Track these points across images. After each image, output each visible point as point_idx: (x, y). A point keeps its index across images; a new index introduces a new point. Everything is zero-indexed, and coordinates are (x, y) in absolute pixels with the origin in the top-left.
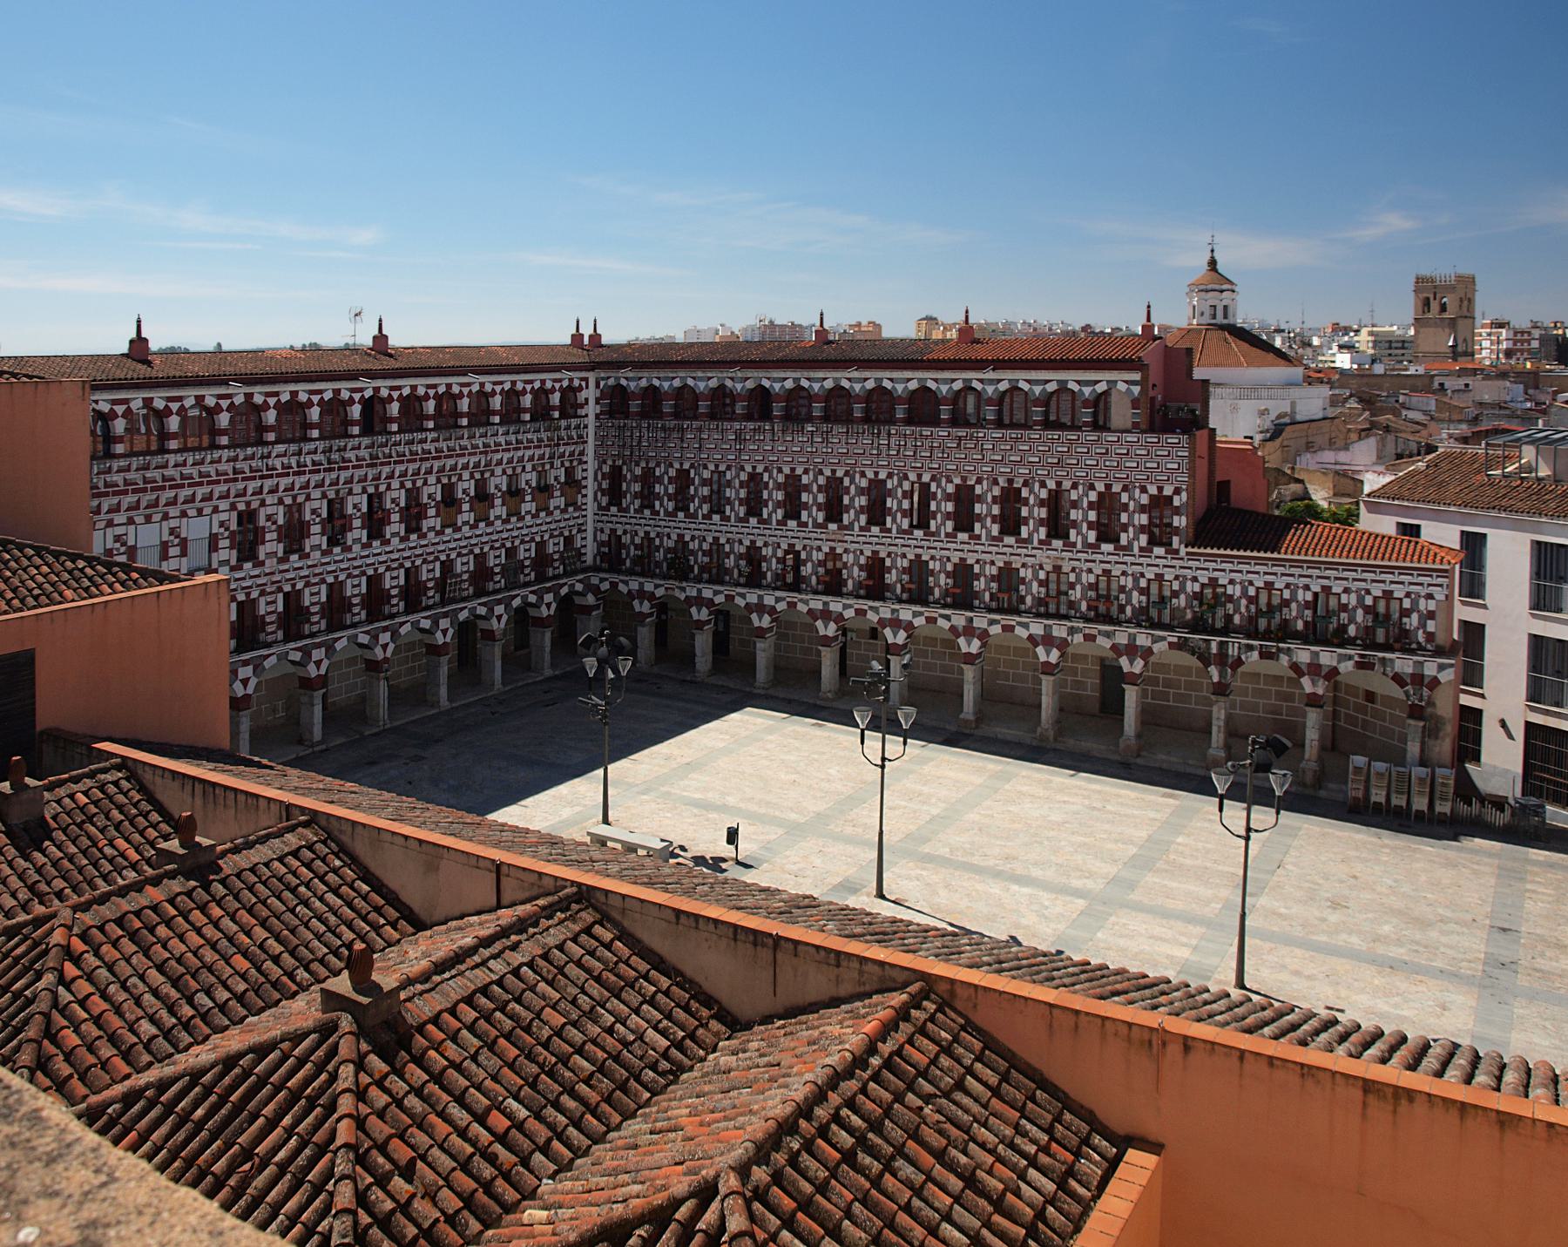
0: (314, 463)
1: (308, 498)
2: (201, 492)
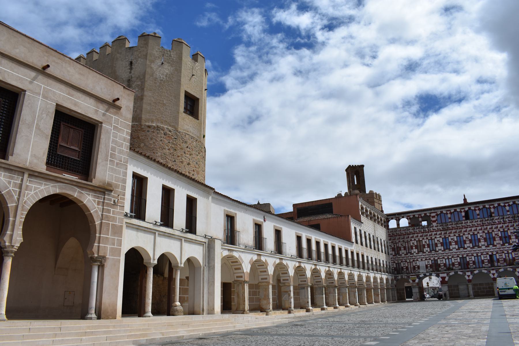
0: (509, 220)
1: (509, 229)
2: (473, 229)
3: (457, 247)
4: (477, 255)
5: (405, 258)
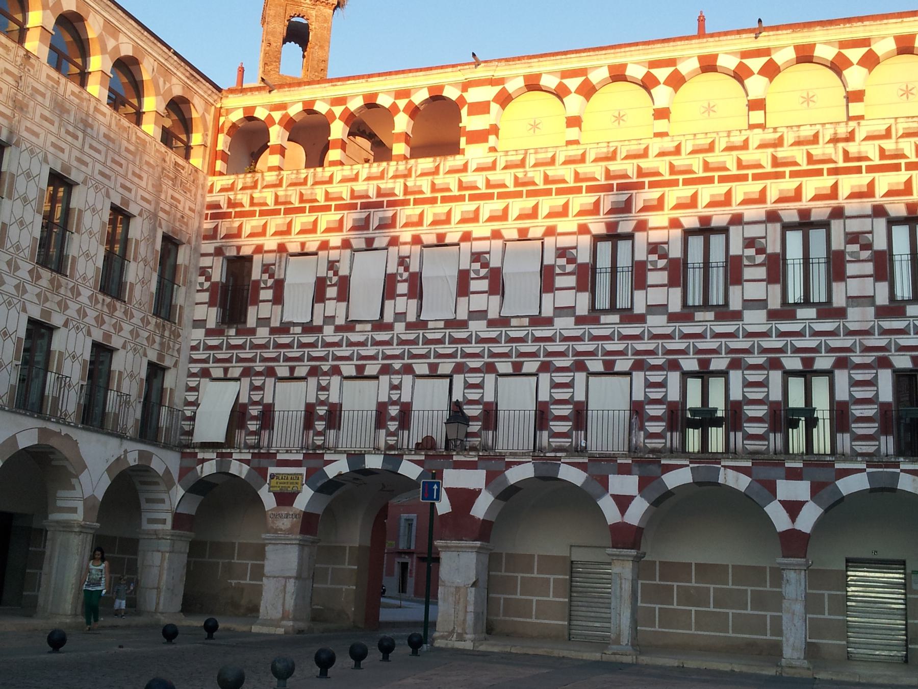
3: (582, 304)
4: (704, 363)
5: (270, 353)
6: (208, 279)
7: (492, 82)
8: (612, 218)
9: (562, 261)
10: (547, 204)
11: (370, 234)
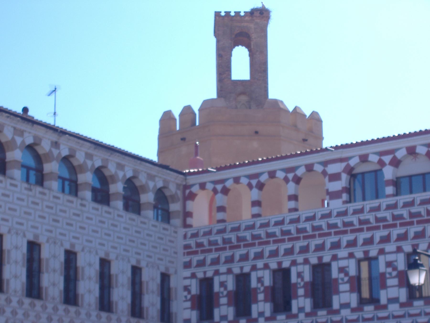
6: (189, 292)
7: (341, 160)
8: (415, 242)
9: (389, 270)
10: (378, 235)
11: (279, 259)
